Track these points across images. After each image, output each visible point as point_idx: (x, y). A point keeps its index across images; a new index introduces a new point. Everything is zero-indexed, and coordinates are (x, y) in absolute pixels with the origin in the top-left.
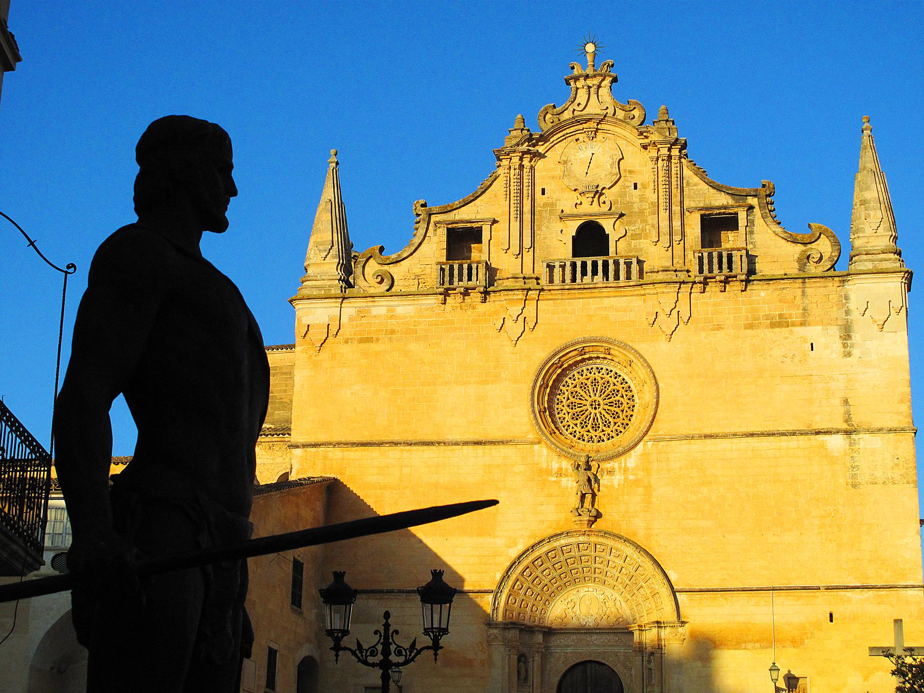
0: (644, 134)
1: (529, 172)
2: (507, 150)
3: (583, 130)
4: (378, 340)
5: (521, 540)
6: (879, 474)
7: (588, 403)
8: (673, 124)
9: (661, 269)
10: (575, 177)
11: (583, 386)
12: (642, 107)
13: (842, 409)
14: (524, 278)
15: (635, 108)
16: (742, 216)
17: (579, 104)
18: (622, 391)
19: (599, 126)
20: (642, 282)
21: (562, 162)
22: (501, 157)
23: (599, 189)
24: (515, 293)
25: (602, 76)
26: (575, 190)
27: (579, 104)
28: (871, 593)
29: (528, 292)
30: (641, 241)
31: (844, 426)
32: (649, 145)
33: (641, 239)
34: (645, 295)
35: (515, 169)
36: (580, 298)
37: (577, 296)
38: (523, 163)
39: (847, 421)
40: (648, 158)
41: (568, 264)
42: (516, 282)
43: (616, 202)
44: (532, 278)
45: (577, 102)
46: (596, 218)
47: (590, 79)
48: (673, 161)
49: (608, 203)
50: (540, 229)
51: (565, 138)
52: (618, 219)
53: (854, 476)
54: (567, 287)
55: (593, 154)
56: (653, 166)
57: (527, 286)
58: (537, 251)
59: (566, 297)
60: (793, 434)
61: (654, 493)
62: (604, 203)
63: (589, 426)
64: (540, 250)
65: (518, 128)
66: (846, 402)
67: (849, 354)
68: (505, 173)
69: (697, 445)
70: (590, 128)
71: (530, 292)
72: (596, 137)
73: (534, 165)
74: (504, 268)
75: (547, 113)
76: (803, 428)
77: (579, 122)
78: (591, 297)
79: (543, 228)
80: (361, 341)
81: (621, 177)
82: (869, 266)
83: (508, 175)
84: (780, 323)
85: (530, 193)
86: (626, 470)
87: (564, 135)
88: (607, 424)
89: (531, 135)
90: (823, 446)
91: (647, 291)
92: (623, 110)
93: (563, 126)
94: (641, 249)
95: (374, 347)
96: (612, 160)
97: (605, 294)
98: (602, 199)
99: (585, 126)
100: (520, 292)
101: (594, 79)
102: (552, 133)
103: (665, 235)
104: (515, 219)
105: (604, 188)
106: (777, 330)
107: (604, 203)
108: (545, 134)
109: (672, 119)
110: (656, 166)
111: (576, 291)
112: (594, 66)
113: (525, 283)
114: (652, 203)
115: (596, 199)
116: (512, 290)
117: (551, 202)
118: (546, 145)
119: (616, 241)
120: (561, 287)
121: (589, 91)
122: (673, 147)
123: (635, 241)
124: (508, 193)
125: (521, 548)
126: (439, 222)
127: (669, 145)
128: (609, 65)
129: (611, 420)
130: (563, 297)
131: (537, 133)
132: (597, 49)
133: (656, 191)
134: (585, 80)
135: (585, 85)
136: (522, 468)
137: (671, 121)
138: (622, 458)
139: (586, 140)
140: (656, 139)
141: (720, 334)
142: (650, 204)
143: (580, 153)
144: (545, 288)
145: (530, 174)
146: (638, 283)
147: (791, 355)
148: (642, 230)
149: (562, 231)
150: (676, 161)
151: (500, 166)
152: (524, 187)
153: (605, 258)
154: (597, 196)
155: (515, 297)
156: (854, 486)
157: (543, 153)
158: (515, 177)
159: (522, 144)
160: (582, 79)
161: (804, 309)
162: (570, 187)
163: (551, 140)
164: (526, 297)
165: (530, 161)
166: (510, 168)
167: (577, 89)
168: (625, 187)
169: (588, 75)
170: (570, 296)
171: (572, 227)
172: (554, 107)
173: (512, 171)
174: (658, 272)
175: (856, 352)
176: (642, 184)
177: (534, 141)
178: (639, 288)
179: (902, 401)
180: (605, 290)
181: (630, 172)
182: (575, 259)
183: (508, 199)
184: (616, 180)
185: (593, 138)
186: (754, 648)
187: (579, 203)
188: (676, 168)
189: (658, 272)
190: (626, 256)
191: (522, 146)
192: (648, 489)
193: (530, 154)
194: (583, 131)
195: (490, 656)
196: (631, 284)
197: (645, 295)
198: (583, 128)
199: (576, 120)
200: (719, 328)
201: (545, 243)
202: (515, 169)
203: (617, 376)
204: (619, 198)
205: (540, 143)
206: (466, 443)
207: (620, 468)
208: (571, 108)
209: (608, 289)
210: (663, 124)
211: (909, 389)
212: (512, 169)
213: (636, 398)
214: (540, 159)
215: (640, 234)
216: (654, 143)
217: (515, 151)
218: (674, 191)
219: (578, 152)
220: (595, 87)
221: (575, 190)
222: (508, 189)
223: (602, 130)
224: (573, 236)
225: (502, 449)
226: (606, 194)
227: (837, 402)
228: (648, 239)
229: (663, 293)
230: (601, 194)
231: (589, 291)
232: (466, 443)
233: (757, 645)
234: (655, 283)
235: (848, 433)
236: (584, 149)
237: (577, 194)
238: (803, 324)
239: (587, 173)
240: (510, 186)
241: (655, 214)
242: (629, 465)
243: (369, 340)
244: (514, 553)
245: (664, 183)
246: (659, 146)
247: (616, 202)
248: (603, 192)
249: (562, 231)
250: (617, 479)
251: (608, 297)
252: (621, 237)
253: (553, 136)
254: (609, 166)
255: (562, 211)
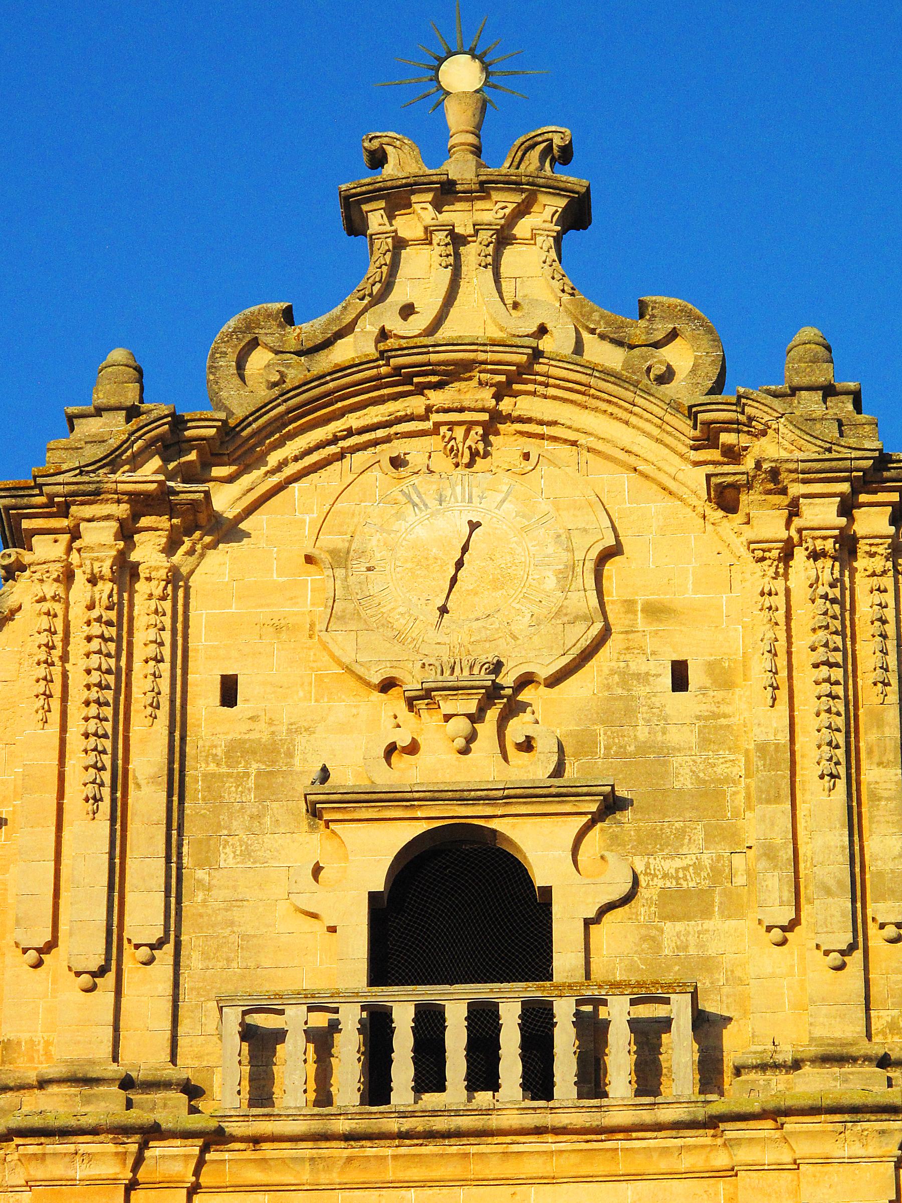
0: (726, 438)
1: (163, 598)
2: (57, 487)
3: (425, 418)
8: (858, 408)
9: (814, 1050)
10: (389, 625)
12: (709, 331)
14: (127, 1083)
15: (673, 335)
17: (407, 311)
19: (506, 405)
20: (719, 1106)
21: (325, 557)
22: (26, 524)
23: (507, 679)
24: (83, 1148)
25: (512, 184)
26: (387, 685)
27: (407, 311)
29: (144, 1146)
30: (708, 924)
32: (749, 486)
33: (706, 913)
34: (732, 1172)
35: (93, 580)
36: (407, 1185)
37: (391, 1172)
38: (134, 557)
40: (743, 551)
42: (87, 1101)
43: (587, 745)
44: (166, 1085)
45: (399, 296)
46: (489, 811)
47: (459, 206)
48: (861, 563)
49: (545, 746)
50: (207, 862)
51: (341, 456)
52: (596, 819)
54: (342, 1126)
55: (474, 526)
56: (768, 584)
57: (135, 1117)
58: (193, 960)
59: (335, 1177)
62: (527, 745)
64: (205, 956)
65: (113, 401)
68: (43, 599)
70: (461, 410)
71: (156, 1150)
72: (486, 454)
73: (184, 571)
74: (24, 1036)
75: (254, 343)
77: (408, 380)
78: (463, 1182)
79: (227, 858)
81: (605, 634)
83: (58, 608)
85: (165, 688)
87: (335, 440)
89: (178, 423)
91: (744, 1155)
92: (619, 343)
93: (329, 398)
94: (707, 963)
96: (565, 556)
97: (533, 1167)
98: (517, 729)
99: (436, 398)
100: (105, 1147)
101: (479, 205)
102: (281, 422)
103: (828, 892)
104: (90, 806)
105: (526, 681)
107: (527, 745)
108: (244, 422)
109: (852, 385)
110: (779, 585)
111: (386, 1150)
112: (477, 151)
113: (129, 1104)
114: (762, 748)
115: (487, 729)
116: (64, 1133)
117: (265, 738)
118: (246, 480)
119: (588, 923)
120: (316, 1126)
121: (457, 255)
122: (863, 498)
123: (680, 926)
124: (56, 688)
127: (845, 487)
128: (549, 148)
130: (324, 1178)
131: (208, 414)
132: (492, 80)
133: (783, 694)
134: (438, 206)
135: (441, 227)
137: (847, 393)
139: (441, 463)
140: (784, 455)
142: (754, 757)
143: (411, 518)
144: (233, 1128)
145: (167, 605)
146: (700, 1113)
148: (716, 873)
149: (317, 870)
150: (879, 564)
151: (23, 568)
152: (137, 665)
153: (532, 990)
154: (492, 715)
155: (81, 1171)
157: (230, 514)
158: (95, 613)
159: (136, 463)
160: (422, 203)
162: (361, 671)
163: (273, 459)
164: (135, 1168)
165: (171, 548)
166: (68, 577)
167: (400, 244)
168: (627, 678)
169: (453, 183)
170: (354, 1175)
172: (288, 317)
173: (80, 591)
174: (796, 1065)
176: (712, 667)
177: (193, 456)
178: (703, 1138)
180: (531, 1144)
181: (655, 611)
182: (383, 995)
183: (55, 717)
184: (584, 643)
185: (474, 454)
187: (403, 740)
188: (877, 598)
189: (796, 1065)
190: (639, 985)
191: (133, 470)
193: (172, 511)
194: (428, 425)
196: (667, 1115)
197: (732, 1172)
198: (429, 409)
199: (397, 370)
201: (232, 923)
202: (93, 580)
204: (600, 729)
205: (217, 472)
208: (369, 326)
209: (550, 1143)
210: (812, 402)
212: (80, 578)
214: (214, 546)
215: (704, 895)
216: (774, 474)
217: (97, 493)
218: (869, 696)
219: (399, 516)
220: (484, 236)
221: (387, 685)
222: (57, 671)
223: (520, 420)
224: (373, 896)
226: (538, 706)
228: (742, 917)
229: (826, 1161)
230: (513, 709)
231: (453, 1148)
234: (788, 1112)
236: (433, 504)
237: (395, 703)
239: (443, 610)
240: (64, 658)
241: (777, 799)
245: (821, 654)
246: (796, 489)
247: (587, 745)
248: (523, 697)
249: (317, 870)
251: (551, 1180)
252: (610, 907)
253: (280, 444)
254: (551, 583)
255: (325, 775)
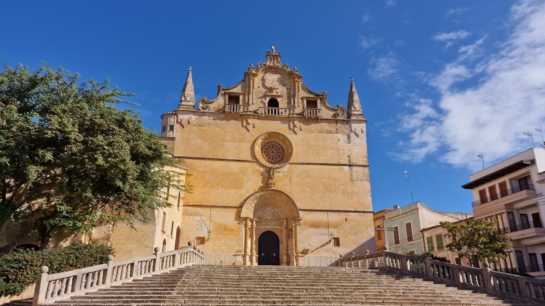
4: (205, 126)
5: (251, 191)
6: (359, 177)
7: (271, 152)
11: (269, 146)
13: (348, 158)
16: (319, 101)
18: (281, 149)
28: (358, 214)
31: (348, 163)
39: (349, 162)
41: (267, 109)
53: (352, 178)
60: (334, 165)
61: (292, 179)
63: (271, 158)
66: (349, 156)
67: (350, 143)
69: (305, 166)
76: (337, 163)
80: (199, 126)
82: (355, 118)
84: (329, 132)
86: (284, 171)
88: (276, 158)
90: (343, 169)
95: (204, 128)
106: (329, 134)
125: (250, 194)
126: (226, 92)
129: (278, 157)
136: (251, 169)
138: (283, 168)
141: (313, 134)
147: (333, 141)
156: (352, 181)
161: (337, 129)
171: (268, 99)
175: (351, 142)
179: (365, 158)
186: (323, 228)
192: (290, 179)
195: (240, 228)
200: (312, 132)
203: (279, 144)
206: (233, 160)
207: (282, 171)
211: (367, 154)
213: (286, 152)
225: (246, 163)
227: (346, 156)
232: (233, 160)
233: (324, 227)
235: (350, 166)
238: (336, 133)
242: (284, 170)
243: (202, 126)
244: (248, 195)
250: (281, 175)
